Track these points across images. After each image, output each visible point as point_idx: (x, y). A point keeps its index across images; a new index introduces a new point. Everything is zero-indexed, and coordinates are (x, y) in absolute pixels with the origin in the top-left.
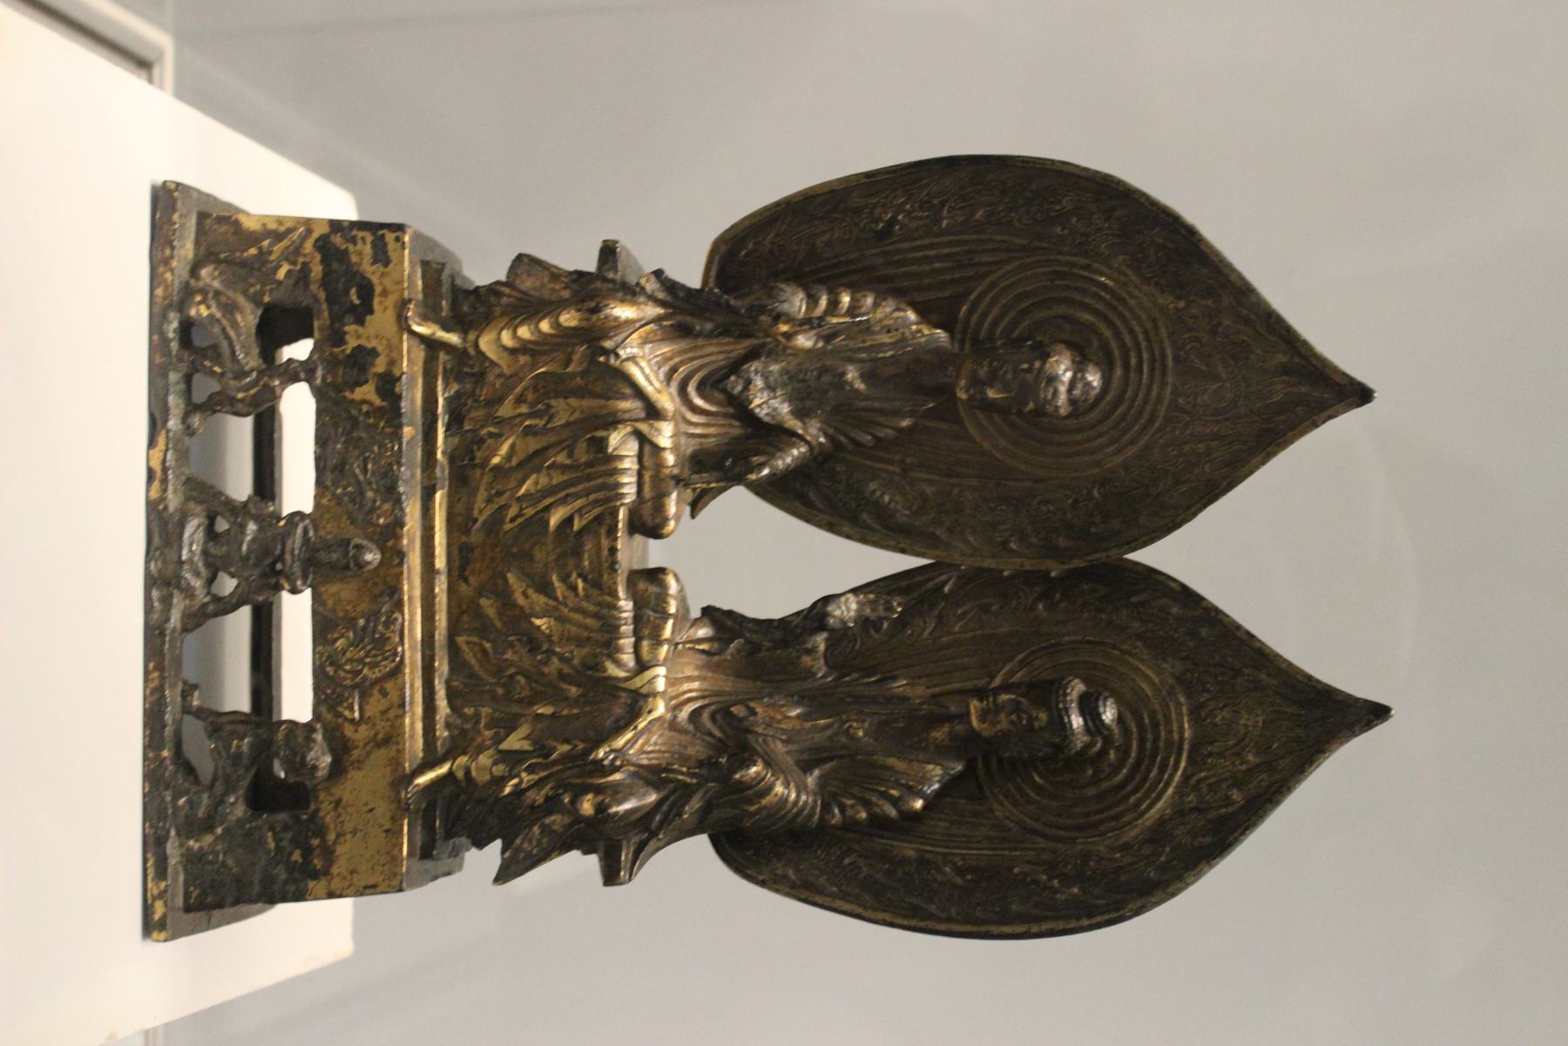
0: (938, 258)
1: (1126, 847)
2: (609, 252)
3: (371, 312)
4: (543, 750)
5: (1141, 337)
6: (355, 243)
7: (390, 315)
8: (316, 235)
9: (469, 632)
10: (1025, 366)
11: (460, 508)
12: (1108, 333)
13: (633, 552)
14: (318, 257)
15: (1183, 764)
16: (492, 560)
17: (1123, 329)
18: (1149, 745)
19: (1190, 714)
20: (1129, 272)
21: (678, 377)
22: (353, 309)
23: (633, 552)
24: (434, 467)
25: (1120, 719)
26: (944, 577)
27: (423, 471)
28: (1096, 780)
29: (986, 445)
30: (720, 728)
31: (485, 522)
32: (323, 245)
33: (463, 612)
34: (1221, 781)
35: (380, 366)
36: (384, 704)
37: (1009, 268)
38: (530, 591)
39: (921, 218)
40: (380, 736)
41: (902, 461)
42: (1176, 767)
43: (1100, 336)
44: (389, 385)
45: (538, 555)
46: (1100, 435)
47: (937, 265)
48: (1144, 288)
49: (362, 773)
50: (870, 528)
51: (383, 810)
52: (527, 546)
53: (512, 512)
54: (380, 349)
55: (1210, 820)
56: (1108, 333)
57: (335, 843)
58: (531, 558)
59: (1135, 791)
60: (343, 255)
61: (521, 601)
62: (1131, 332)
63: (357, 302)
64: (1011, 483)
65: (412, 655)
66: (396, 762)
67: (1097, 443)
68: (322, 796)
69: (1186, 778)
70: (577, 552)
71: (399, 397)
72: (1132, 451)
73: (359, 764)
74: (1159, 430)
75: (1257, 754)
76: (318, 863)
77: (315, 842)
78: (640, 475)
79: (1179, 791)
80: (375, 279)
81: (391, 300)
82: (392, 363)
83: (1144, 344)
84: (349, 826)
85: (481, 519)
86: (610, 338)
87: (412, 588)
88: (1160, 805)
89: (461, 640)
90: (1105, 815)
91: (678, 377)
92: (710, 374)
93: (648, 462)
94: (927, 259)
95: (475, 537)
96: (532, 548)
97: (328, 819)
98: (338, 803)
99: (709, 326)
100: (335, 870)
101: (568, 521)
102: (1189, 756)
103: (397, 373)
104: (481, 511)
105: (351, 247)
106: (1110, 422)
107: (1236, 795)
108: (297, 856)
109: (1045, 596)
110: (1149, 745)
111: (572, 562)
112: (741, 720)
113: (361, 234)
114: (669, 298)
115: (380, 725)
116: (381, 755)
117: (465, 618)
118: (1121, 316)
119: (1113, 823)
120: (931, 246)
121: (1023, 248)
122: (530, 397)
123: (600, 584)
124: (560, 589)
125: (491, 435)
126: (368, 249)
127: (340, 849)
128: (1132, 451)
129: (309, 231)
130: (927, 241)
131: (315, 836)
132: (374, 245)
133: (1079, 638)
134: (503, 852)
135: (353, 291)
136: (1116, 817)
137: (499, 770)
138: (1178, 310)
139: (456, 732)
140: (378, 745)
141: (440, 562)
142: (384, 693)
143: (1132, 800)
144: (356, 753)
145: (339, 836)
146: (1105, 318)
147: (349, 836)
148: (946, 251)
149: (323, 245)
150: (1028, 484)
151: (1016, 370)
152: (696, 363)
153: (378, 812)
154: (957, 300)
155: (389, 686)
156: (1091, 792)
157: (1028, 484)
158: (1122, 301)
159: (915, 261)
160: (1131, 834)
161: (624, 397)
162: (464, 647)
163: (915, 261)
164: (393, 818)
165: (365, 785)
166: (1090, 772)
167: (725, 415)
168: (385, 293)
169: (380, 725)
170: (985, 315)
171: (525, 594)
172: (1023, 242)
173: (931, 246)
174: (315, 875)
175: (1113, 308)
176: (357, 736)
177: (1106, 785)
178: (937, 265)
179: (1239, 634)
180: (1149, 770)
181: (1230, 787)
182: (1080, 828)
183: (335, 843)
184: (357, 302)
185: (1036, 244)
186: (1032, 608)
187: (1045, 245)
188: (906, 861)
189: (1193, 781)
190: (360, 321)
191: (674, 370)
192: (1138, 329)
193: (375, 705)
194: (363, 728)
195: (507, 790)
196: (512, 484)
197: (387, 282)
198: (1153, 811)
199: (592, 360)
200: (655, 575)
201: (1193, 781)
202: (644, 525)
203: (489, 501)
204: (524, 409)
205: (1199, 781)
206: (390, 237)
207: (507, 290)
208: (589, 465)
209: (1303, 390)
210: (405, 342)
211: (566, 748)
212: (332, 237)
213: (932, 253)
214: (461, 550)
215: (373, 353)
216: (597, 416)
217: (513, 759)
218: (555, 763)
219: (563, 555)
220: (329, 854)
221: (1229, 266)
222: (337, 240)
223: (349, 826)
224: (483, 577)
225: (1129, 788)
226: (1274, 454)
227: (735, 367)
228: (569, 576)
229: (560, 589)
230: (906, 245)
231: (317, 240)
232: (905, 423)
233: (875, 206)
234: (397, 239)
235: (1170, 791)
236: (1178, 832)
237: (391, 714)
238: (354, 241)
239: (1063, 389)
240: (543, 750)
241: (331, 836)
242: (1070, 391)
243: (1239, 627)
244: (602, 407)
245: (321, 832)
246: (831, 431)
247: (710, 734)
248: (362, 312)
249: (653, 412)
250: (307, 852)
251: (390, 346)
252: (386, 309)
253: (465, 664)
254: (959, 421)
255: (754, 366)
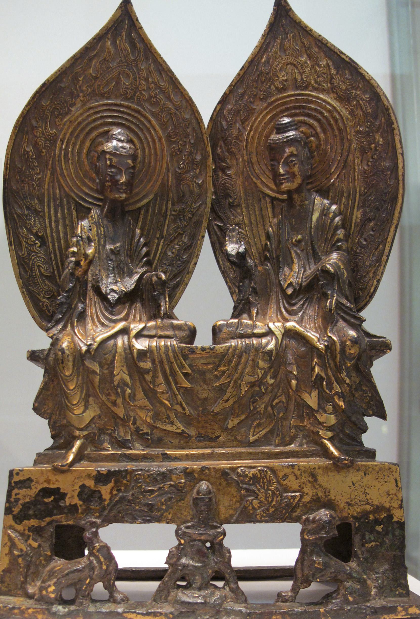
0: (56, 216)
1: (352, 113)
2: (33, 356)
3: (59, 489)
4: (318, 383)
5: (98, 116)
6: (19, 499)
7: (60, 477)
8: (13, 523)
9: (247, 435)
10: (108, 162)
11: (175, 441)
12: (95, 133)
13: (204, 340)
14: (25, 522)
15: (307, 92)
16: (206, 422)
17: (93, 125)
18: (298, 111)
19: (281, 93)
20: (65, 120)
21: (106, 323)
22: (56, 501)
23: (204, 340)
24: (151, 455)
25: (287, 116)
26: (215, 227)
27: (153, 461)
28: (316, 135)
29: (151, 197)
30: (300, 301)
31: (185, 427)
32: (18, 519)
33: (236, 439)
34: (316, 71)
35: (90, 483)
36: (292, 478)
37: (62, 181)
38: (225, 398)
39: (35, 221)
40: (310, 479)
41: (158, 238)
42: (309, 95)
43: (97, 136)
44: (102, 478)
45: (204, 395)
46: (146, 138)
47: (59, 216)
48: (73, 113)
49: (332, 491)
50: (191, 253)
51: (353, 476)
52: (199, 402)
53: (179, 409)
54: (81, 484)
55: (337, 73)
56: (95, 133)
57: (372, 505)
58: (205, 399)
59: (321, 113)
60: (26, 507)
61: (231, 402)
62: (95, 120)
63: (52, 498)
64: (170, 183)
65: (261, 464)
66: (326, 469)
67: (150, 140)
68: (345, 514)
69: (315, 89)
70: (203, 373)
71: (109, 471)
72: (154, 122)
73: (327, 492)
74: (144, 109)
75: (302, 56)
76: (383, 515)
77: (371, 517)
78: (161, 337)
79: (323, 91)
80: (40, 487)
81: (53, 478)
82: (89, 476)
83: (101, 115)
84: (362, 497)
85: (182, 428)
86: (81, 348)
87: (224, 464)
88: (329, 100)
89: (252, 439)
90: (335, 127)
91: (106, 323)
92: (106, 309)
93: (153, 333)
94: (57, 221)
95: (192, 432)
96: (200, 399)
97: (359, 510)
98: (349, 504)
99: (80, 306)
100: (387, 505)
101: (186, 375)
102: (303, 90)
103: (95, 473)
104: (178, 428)
105: (21, 502)
106: (140, 133)
107: (323, 63)
108: (379, 528)
109: (223, 170)
110: (298, 111)
111: (208, 376)
112: (295, 289)
113: (13, 496)
114: (62, 324)
115: (303, 479)
116: (321, 479)
117: (239, 438)
118: (87, 125)
119: (339, 121)
120: (50, 218)
121: (52, 174)
122: (113, 398)
123: (222, 358)
124: (223, 380)
125: (134, 423)
126: (23, 492)
127: (376, 503)
128: (154, 122)
129: (11, 527)
130: (47, 220)
131: (368, 518)
132: (20, 488)
133: (245, 152)
134: (369, 416)
135: (46, 500)
136: (336, 121)
137: (329, 407)
138: (84, 96)
139: (304, 441)
140: (316, 480)
141: (208, 451)
142: (285, 476)
143: (326, 114)
144: (320, 494)
145: (368, 503)
146: (88, 133)
147: (368, 497)
148: (52, 212)
149: (18, 519)
150: (170, 174)
151: (111, 166)
152: (99, 314)
153: (354, 480)
154: (78, 205)
155: (281, 474)
156: (322, 136)
157: (170, 174)
158: (79, 123)
159: (57, 227)
160: (345, 112)
161: (116, 345)
162: (256, 437)
163: (57, 227)
164: (358, 470)
165: (340, 487)
166: (312, 138)
167: (130, 308)
168: (48, 481)
169: (303, 479)
170: (87, 194)
171: (227, 401)
172: (49, 174)
173: (50, 218)
174: (390, 517)
175: (83, 129)
176: (311, 494)
177: (319, 130)
178: (59, 216)
179: (242, 74)
180: (311, 109)
181: (319, 66)
182: (342, 139)
183: (372, 505)
184: (52, 498)
185: (50, 167)
186: (229, 176)
187: (50, 163)
188: (364, 214)
189: (316, 86)
190: (65, 495)
191: (103, 324)
192: (94, 117)
193: (292, 483)
194: (306, 490)
195: (342, 404)
196: (163, 410)
197: (42, 480)
198: (333, 103)
199: (93, 358)
200: (216, 331)
201: (316, 86)
202: (188, 336)
203: (172, 423)
204: (119, 401)
205: (316, 82)
206: (16, 479)
207: (54, 417)
208: (153, 362)
209: (124, 33)
210: (79, 472)
211: (317, 369)
212: (14, 513)
213: (53, 219)
214: (200, 441)
215: (83, 487)
216: (126, 358)
217: (324, 399)
218: (327, 374)
219: (205, 381)
220: (378, 509)
221: (61, 68)
222: (16, 510)
223: (362, 497)
224: (216, 427)
225: (320, 117)
226: (155, 49)
227: (103, 297)
228: (216, 376)
229: (223, 380)
230: (48, 229)
231: (16, 523)
232: (138, 231)
233: (27, 243)
234: (17, 474)
235: (321, 96)
236: (344, 88)
237: (298, 473)
238: (17, 500)
239: (120, 144)
240: (318, 383)
241: (368, 507)
242: (122, 141)
243: (239, 74)
244: (121, 355)
245: (365, 514)
246: (141, 264)
247: (303, 305)
248: (58, 494)
249: (125, 331)
250: (377, 522)
251: (79, 478)
252: (57, 481)
253: (265, 435)
254: (140, 209)
255: (103, 289)
